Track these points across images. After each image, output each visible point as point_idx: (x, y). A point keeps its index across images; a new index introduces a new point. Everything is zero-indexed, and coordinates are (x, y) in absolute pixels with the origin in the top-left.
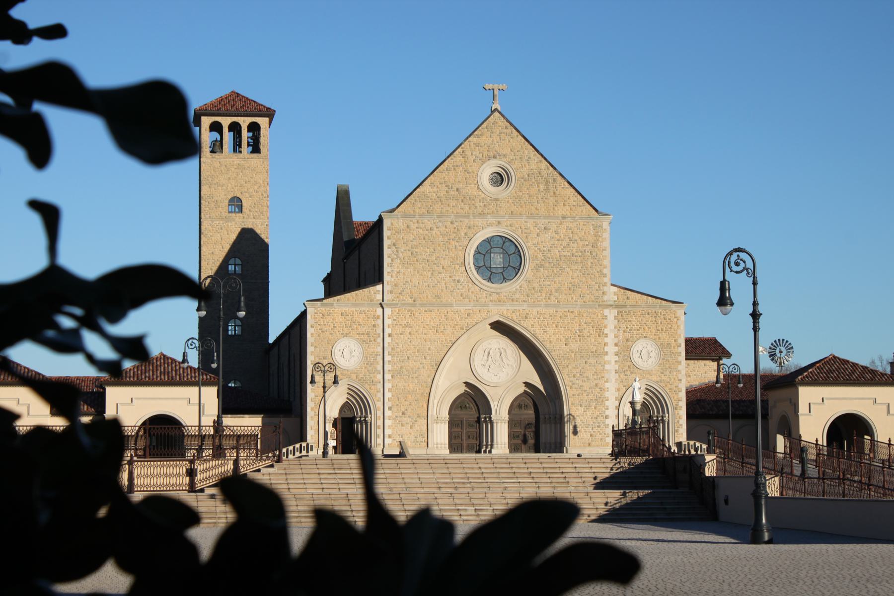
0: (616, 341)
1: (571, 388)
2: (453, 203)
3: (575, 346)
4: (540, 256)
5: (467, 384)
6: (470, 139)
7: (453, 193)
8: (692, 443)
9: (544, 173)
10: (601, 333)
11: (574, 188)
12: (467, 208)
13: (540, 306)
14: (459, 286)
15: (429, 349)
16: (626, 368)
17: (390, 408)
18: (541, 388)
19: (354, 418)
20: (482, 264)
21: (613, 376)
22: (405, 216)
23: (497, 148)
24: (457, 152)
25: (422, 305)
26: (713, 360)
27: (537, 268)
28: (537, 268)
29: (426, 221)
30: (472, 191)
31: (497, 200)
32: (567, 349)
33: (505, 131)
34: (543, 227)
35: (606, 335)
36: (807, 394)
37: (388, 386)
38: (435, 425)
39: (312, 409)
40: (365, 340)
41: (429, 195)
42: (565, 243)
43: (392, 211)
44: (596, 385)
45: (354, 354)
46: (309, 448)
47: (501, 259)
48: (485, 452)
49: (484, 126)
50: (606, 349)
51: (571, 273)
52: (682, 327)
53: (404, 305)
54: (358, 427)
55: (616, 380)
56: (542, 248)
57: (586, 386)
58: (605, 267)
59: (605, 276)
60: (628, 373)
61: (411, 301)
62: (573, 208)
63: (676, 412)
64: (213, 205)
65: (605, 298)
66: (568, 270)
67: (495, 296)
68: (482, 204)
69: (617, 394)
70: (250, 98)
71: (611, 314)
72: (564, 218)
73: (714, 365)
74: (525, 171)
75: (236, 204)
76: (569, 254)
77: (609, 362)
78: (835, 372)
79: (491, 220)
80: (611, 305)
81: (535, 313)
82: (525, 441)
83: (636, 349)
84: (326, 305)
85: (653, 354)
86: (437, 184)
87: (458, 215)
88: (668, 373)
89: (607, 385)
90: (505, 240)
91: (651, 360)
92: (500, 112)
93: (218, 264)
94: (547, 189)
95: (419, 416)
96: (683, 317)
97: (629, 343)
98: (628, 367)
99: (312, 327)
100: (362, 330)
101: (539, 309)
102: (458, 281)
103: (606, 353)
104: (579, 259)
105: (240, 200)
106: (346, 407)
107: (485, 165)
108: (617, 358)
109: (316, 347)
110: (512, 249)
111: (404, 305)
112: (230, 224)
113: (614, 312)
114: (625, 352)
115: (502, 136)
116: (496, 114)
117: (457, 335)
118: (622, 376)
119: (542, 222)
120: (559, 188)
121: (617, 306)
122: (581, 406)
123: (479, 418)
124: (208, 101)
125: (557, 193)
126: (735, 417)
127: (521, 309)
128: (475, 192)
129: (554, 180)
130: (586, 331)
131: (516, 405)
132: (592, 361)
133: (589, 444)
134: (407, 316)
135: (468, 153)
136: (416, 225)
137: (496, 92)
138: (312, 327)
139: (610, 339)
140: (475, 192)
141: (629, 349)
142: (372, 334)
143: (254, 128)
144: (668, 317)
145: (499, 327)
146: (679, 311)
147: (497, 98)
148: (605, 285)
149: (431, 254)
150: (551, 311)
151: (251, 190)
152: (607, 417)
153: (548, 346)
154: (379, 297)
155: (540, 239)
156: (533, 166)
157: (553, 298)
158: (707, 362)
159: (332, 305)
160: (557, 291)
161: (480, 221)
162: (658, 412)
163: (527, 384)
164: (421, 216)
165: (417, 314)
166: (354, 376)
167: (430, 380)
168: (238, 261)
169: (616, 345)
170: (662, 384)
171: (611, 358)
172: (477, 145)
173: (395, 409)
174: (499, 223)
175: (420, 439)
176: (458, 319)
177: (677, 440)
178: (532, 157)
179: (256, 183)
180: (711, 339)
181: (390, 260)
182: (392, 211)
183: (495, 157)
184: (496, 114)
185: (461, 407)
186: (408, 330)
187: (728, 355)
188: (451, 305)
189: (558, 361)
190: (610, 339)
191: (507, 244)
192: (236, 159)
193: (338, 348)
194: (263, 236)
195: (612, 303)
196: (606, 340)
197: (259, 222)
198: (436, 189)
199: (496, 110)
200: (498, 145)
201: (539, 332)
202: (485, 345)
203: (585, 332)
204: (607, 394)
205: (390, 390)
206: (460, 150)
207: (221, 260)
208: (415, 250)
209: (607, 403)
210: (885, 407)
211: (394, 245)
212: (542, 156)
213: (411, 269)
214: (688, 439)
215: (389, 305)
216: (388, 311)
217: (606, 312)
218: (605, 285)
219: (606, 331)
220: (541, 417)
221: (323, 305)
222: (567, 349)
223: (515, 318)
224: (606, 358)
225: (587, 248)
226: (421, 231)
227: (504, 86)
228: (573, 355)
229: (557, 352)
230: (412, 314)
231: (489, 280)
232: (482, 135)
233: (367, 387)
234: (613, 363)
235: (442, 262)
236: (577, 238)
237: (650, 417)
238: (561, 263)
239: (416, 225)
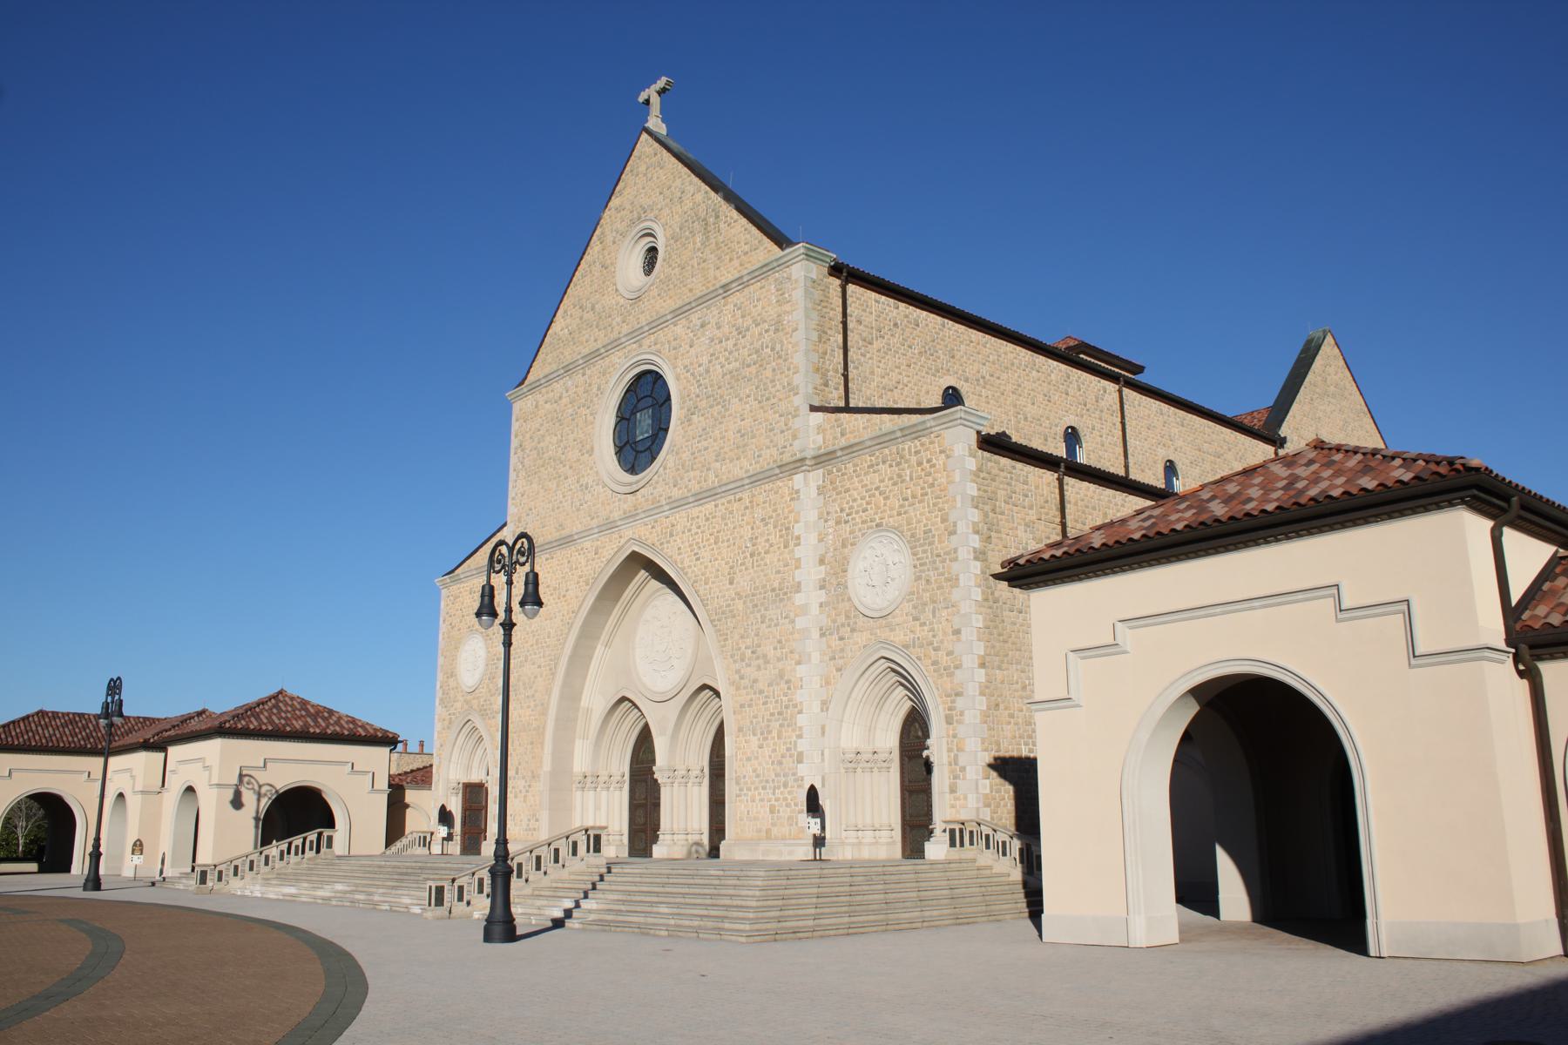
16: (842, 619)
21: (813, 646)
34: (699, 323)
42: (730, 343)
43: (522, 383)
44: (781, 676)
50: (799, 575)
60: (846, 631)
89: (801, 670)
139: (807, 550)
157: (711, 475)
169: (822, 562)
171: (811, 597)
190: (807, 550)
204: (799, 696)
224: (799, 599)
225: (766, 338)
227: (661, 83)
234: (815, 609)
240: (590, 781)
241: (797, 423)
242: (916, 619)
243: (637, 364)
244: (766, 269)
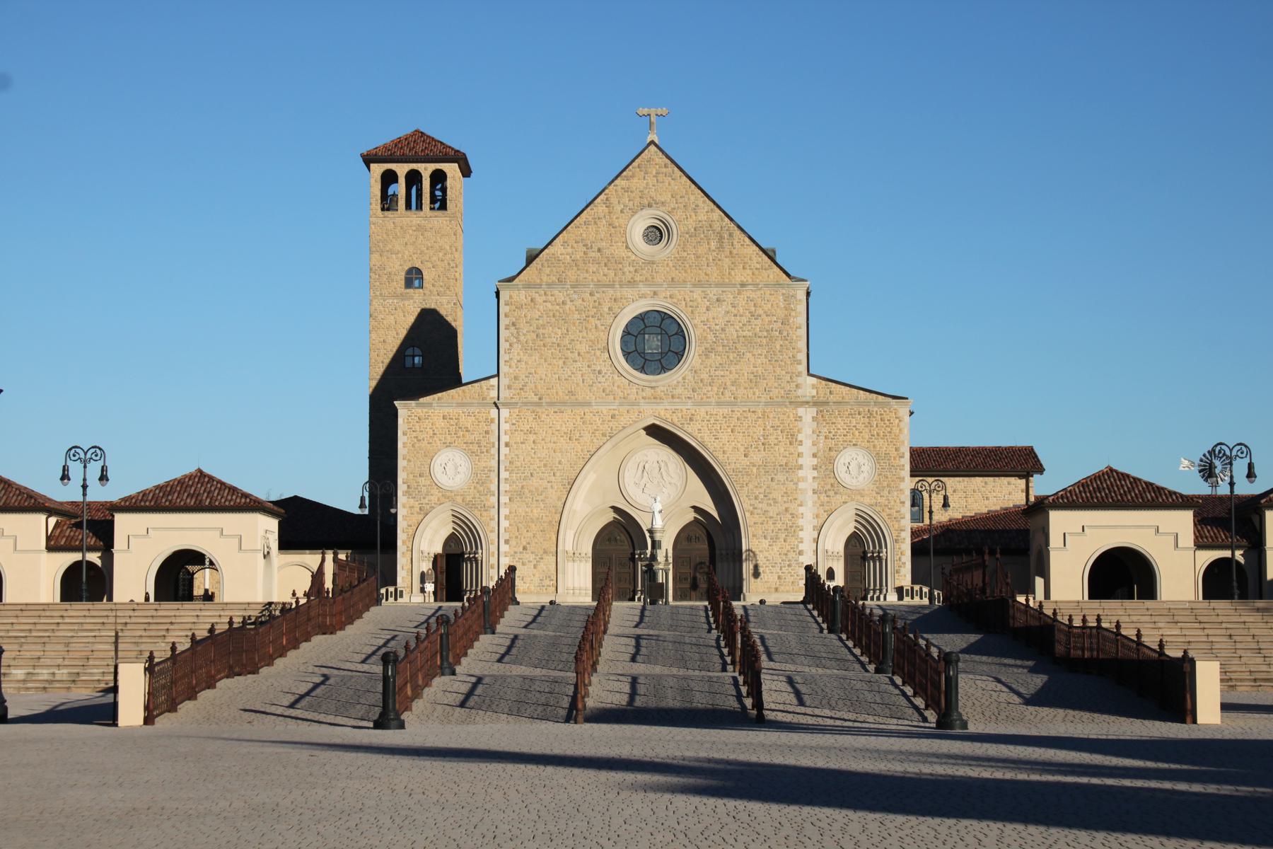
0: (814, 450)
1: (752, 513)
2: (592, 268)
3: (757, 457)
4: (711, 337)
5: (615, 509)
6: (616, 182)
8: (917, 588)
9: (717, 226)
10: (793, 439)
11: (758, 245)
12: (612, 274)
13: (709, 404)
14: (601, 379)
15: (560, 463)
17: (507, 542)
18: (715, 514)
19: (463, 554)
20: (633, 348)
21: (810, 499)
22: (528, 286)
23: (653, 194)
24: (598, 200)
25: (551, 404)
26: (1020, 477)
27: (706, 353)
28: (706, 353)
29: (556, 292)
30: (620, 252)
31: (653, 263)
32: (746, 461)
33: (664, 170)
35: (801, 443)
36: (1059, 521)
37: (504, 511)
38: (570, 564)
39: (404, 542)
40: (474, 450)
41: (561, 257)
42: (744, 320)
43: (511, 279)
44: (787, 510)
45: (459, 469)
46: (398, 594)
47: (656, 343)
48: (872, 599)
50: (800, 461)
51: (752, 360)
52: (906, 431)
53: (525, 404)
54: (466, 567)
55: (814, 503)
56: (713, 327)
57: (773, 511)
58: (800, 351)
59: (799, 363)
60: (831, 493)
61: (536, 399)
63: (897, 546)
64: (384, 278)
65: (800, 392)
66: (749, 355)
67: (648, 392)
68: (632, 269)
69: (815, 522)
70: (437, 137)
71: (807, 414)
72: (743, 285)
73: (1021, 483)
74: (691, 224)
75: (414, 277)
77: (804, 479)
78: (1110, 490)
79: (645, 290)
80: (807, 403)
81: (703, 413)
82: (694, 586)
83: (842, 461)
84: (423, 405)
85: (866, 468)
86: (572, 242)
87: (599, 285)
89: (801, 510)
90: (664, 316)
91: (862, 476)
92: (656, 145)
93: (391, 355)
94: (721, 247)
95: (545, 552)
96: (907, 418)
98: (830, 485)
99: (404, 434)
100: (469, 438)
101: (708, 408)
102: (600, 372)
103: (801, 467)
104: (764, 341)
105: (419, 272)
106: (452, 540)
107: (636, 217)
108: (815, 474)
109: (409, 461)
110: (674, 329)
111: (525, 404)
112: (406, 303)
114: (826, 465)
115: (661, 177)
116: (652, 148)
117: (597, 443)
118: (823, 497)
119: (713, 292)
120: (737, 246)
121: (815, 404)
123: (633, 554)
124: (380, 143)
125: (735, 252)
126: (937, 553)
127: (684, 408)
128: (622, 252)
129: (731, 235)
130: (773, 438)
131: (684, 537)
132: (781, 477)
133: (776, 590)
134: (531, 419)
135: (614, 200)
136: (544, 298)
137: (653, 118)
138: (404, 434)
139: (806, 448)
140: (622, 252)
141: (832, 461)
143: (439, 178)
144: (887, 417)
145: (655, 431)
146: (903, 411)
147: (655, 127)
149: (563, 336)
150: (726, 410)
151: (435, 258)
152: (801, 553)
153: (721, 457)
154: (494, 394)
155: (711, 314)
156: (702, 217)
157: (727, 394)
158: (1012, 480)
159: (430, 405)
161: (628, 292)
162: (874, 547)
163: (696, 509)
164: (549, 285)
165: (544, 416)
166: (459, 499)
167: (560, 504)
168: (417, 351)
169: (814, 455)
170: (878, 509)
171: (807, 473)
172: (626, 190)
173: (513, 542)
174: (655, 293)
175: (547, 582)
176: (599, 423)
177: (898, 584)
178: (701, 205)
179: (441, 249)
180: (1026, 448)
181: (507, 345)
182: (511, 279)
183: (650, 206)
184: (652, 148)
185: (609, 540)
186: (532, 437)
187: (1041, 470)
188: (589, 404)
189: (734, 478)
190: (806, 448)
191: (667, 321)
192: (414, 218)
193: (438, 462)
194: (449, 319)
195: (808, 399)
196: (800, 449)
197: (444, 300)
198: (570, 250)
199: (652, 142)
200: (658, 188)
201: (708, 439)
202: (639, 457)
203: (772, 440)
204: (800, 522)
205: (506, 518)
206: (602, 197)
207: (395, 350)
208: (541, 331)
209: (801, 534)
210: (1172, 538)
211: (514, 324)
213: (536, 356)
214: (914, 582)
215: (506, 405)
216: (505, 412)
217: (801, 411)
219: (800, 437)
220: (717, 552)
221: (418, 405)
222: (746, 461)
223: (676, 420)
224: (801, 473)
225: (775, 326)
226: (549, 305)
227: (664, 111)
228: (755, 470)
229: (733, 466)
230: (537, 417)
231: (642, 370)
232: (633, 176)
233: (476, 513)
234: (810, 480)
235: (578, 346)
236: (761, 312)
237: (865, 553)
238: (738, 346)
239: (544, 298)
240: (574, 556)
241: (800, 380)
243: (654, 305)
244: (779, 285)
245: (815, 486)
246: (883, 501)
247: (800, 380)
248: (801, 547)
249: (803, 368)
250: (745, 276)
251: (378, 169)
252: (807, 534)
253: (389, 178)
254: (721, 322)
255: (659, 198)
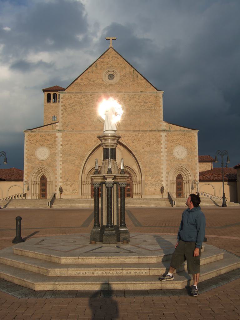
6: (99, 60)
7: (91, 82)
10: (159, 143)
22: (69, 93)
24: (93, 65)
32: (143, 150)
42: (142, 104)
49: (105, 54)
50: (162, 150)
59: (161, 118)
61: (72, 130)
62: (146, 88)
69: (167, 171)
76: (144, 108)
88: (190, 161)
89: (162, 166)
97: (172, 148)
113: (165, 134)
114: (170, 152)
116: (111, 49)
118: (169, 162)
122: (150, 176)
125: (139, 82)
129: (137, 77)
132: (155, 156)
135: (98, 65)
137: (111, 40)
141: (172, 150)
142: (53, 145)
148: (161, 122)
150: (136, 133)
152: (162, 181)
160: (139, 125)
172: (102, 62)
184: (111, 49)
186: (70, 142)
192: (55, 104)
196: (162, 146)
199: (111, 47)
203: (152, 143)
204: (162, 171)
209: (162, 175)
211: (64, 105)
212: (132, 66)
217: (162, 133)
218: (161, 122)
222: (143, 150)
224: (162, 154)
234: (165, 157)
241: (161, 123)
242: (188, 161)
245: (167, 158)
246: (190, 164)
247: (161, 123)
248: (162, 179)
249: (162, 119)
250: (143, 90)
251: (46, 93)
252: (164, 175)
253: (49, 96)
254: (135, 104)
255: (114, 65)
